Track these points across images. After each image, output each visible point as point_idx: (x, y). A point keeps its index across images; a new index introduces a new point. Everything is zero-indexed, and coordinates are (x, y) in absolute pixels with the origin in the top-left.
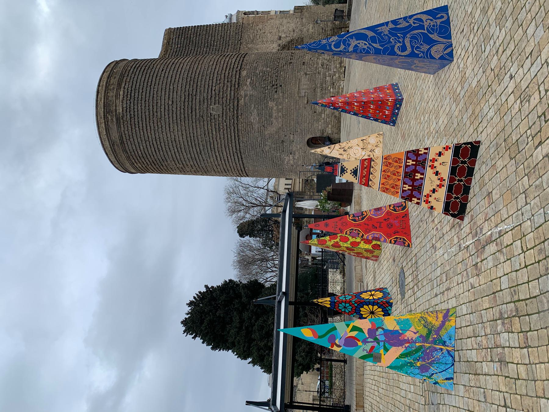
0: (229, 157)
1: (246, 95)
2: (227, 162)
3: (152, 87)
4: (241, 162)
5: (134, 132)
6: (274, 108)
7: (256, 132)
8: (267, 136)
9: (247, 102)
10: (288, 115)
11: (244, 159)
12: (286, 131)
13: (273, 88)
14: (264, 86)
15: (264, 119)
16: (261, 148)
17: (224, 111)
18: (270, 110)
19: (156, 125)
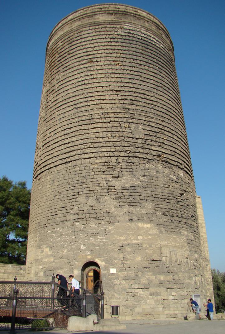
0: (70, 145)
1: (157, 172)
2: (60, 143)
3: (157, 65)
4: (59, 162)
5: (104, 37)
6: (143, 211)
9: (149, 172)
11: (64, 165)
16: (82, 190)
19: (114, 59)
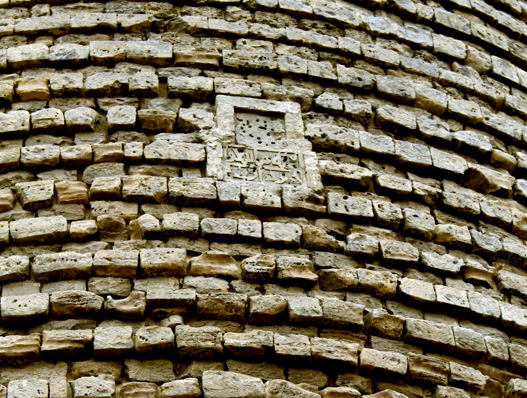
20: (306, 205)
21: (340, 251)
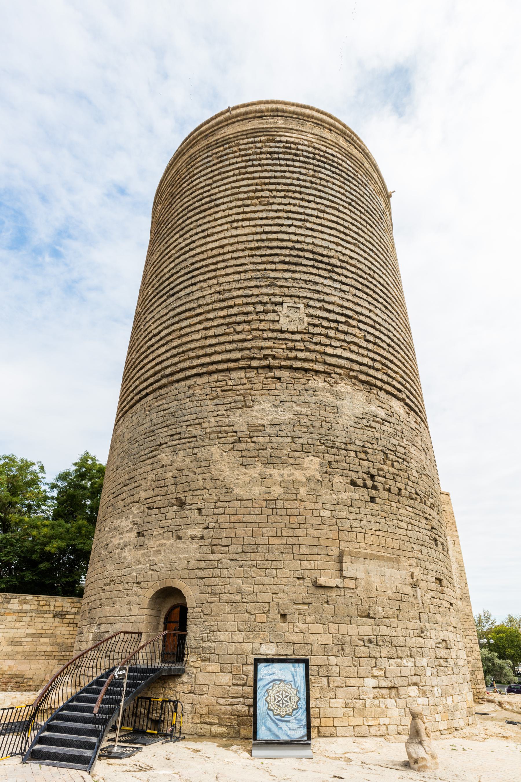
1: (337, 395)
6: (299, 475)
7: (218, 418)
8: (202, 453)
10: (272, 519)
12: (216, 511)
13: (365, 476)
14: (370, 451)
15: (261, 440)
17: (289, 336)
18: (292, 461)
20: (304, 331)
21: (311, 342)
